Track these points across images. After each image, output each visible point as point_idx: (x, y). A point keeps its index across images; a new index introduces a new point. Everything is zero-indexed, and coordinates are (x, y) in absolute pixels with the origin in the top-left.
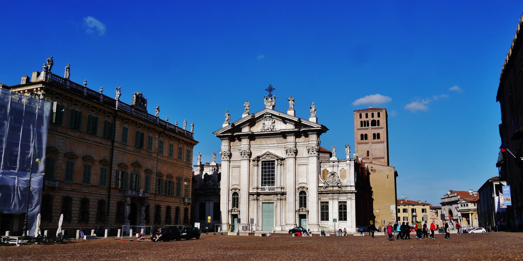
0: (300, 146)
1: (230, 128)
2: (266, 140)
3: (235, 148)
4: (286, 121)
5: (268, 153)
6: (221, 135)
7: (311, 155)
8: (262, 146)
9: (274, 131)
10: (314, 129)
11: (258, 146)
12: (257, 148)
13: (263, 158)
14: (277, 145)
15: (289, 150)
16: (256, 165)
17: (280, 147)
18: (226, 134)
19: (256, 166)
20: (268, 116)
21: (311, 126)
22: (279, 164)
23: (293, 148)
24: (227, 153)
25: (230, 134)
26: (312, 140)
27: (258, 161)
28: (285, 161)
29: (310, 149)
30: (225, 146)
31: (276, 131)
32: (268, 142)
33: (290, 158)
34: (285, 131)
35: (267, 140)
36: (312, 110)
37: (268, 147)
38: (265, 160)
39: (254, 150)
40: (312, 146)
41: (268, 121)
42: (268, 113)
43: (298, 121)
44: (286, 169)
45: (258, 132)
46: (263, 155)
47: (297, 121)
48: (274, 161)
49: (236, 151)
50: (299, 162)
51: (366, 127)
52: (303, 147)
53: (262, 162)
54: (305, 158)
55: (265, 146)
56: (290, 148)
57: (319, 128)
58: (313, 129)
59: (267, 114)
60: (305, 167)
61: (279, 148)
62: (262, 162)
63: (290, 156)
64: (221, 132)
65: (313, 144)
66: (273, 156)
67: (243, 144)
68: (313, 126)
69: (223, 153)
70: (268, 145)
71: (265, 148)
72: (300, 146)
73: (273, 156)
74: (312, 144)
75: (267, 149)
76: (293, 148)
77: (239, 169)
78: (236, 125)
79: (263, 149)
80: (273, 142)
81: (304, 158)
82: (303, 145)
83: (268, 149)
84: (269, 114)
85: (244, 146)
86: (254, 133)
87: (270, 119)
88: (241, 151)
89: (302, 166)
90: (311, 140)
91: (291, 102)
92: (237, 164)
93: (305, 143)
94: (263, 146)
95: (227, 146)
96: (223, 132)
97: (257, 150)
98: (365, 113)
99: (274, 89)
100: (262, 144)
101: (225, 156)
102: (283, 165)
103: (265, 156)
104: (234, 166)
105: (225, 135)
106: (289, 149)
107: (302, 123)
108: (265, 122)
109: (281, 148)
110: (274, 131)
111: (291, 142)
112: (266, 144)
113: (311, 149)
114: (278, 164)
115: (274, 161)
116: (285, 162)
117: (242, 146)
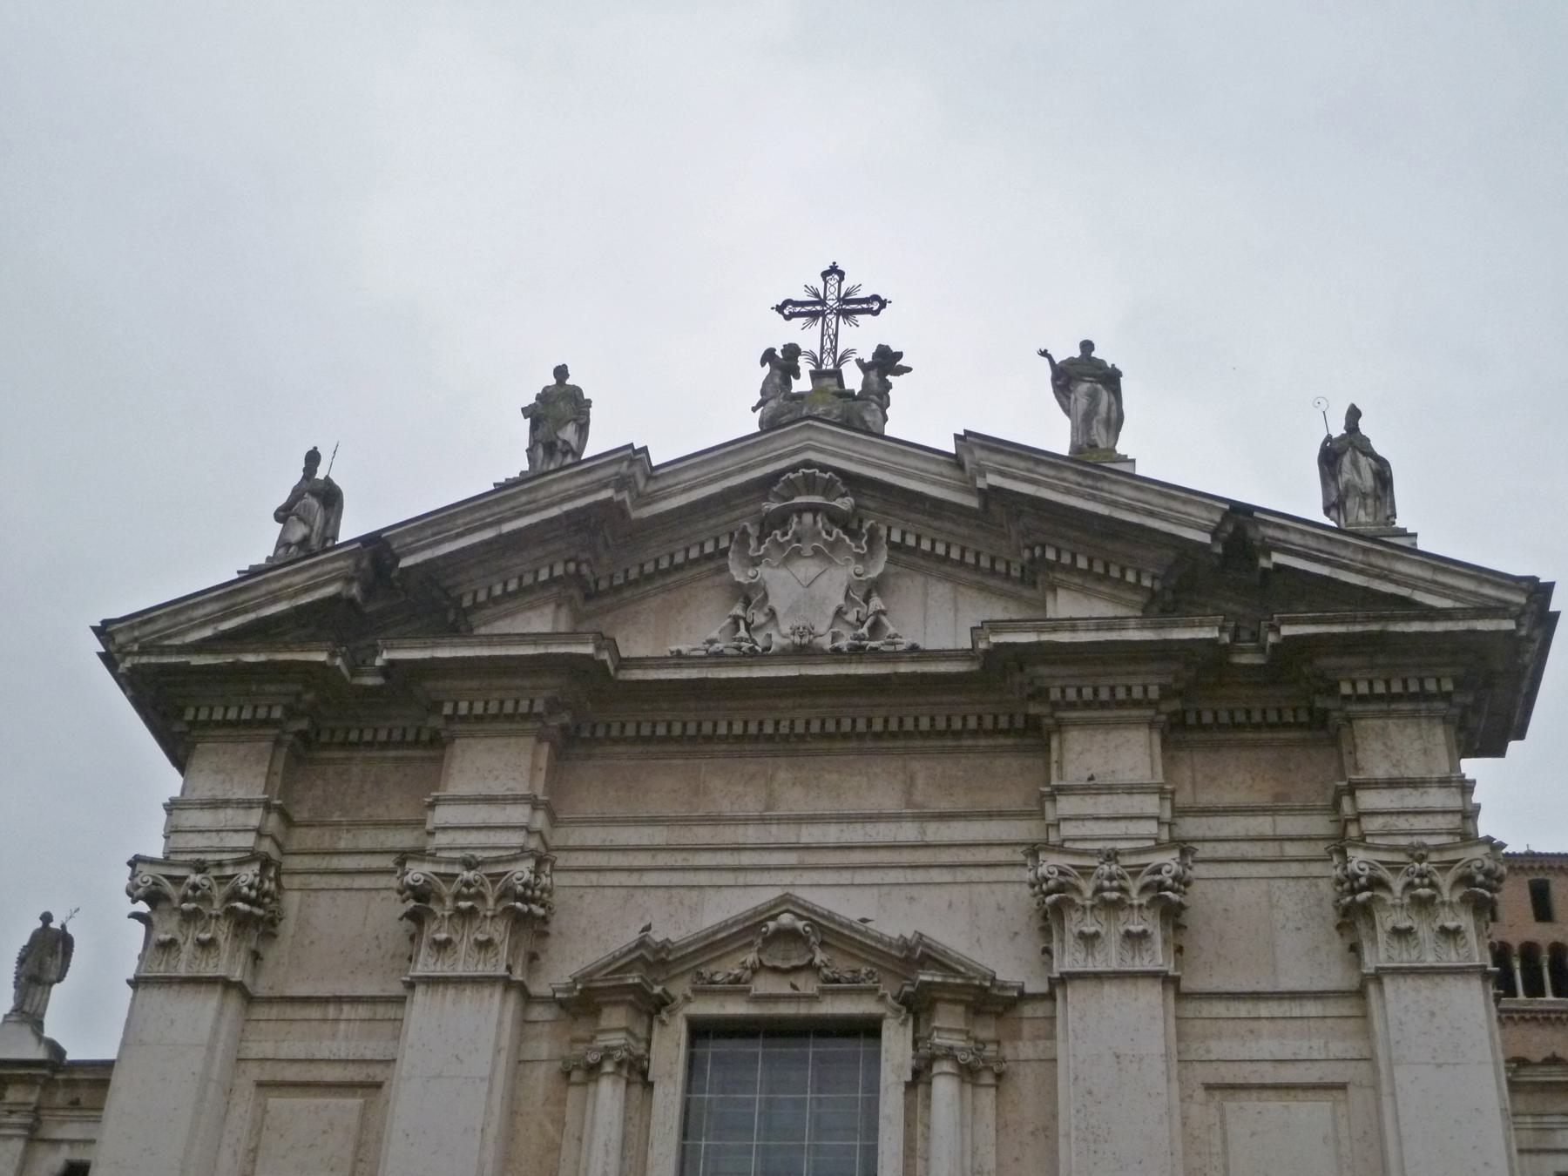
0: (1223, 850)
1: (330, 590)
2: (772, 778)
3: (342, 845)
4: (1051, 555)
5: (786, 919)
6: (197, 660)
7: (1404, 956)
8: (703, 835)
9: (895, 657)
10: (1439, 627)
11: (659, 836)
12: (643, 860)
13: (706, 989)
14: (908, 832)
15: (1087, 887)
16: (608, 1053)
17: (946, 857)
18: (262, 658)
19: (608, 1067)
20: (814, 509)
21: (1393, 596)
22: (949, 1054)
23: (1156, 859)
24: (226, 889)
25: (322, 657)
26: (1395, 773)
27: (653, 1007)
28: (1016, 1036)
29: (1384, 873)
30: (215, 804)
31: (915, 653)
32: (795, 799)
33: (1110, 990)
34: (1045, 637)
35: (782, 775)
36: (1346, 475)
37: (791, 858)
38: (736, 1008)
39: (594, 878)
40: (1403, 841)
41: (806, 569)
42: (824, 468)
43: (1214, 534)
44: (1048, 1130)
45: (679, 659)
46: (714, 945)
47: (1206, 538)
48: (870, 1029)
49: (346, 882)
50: (1218, 1049)
51: (1550, 997)
52: (1262, 869)
53: (701, 1031)
54: (1312, 1008)
55: (751, 834)
56: (1112, 856)
57: (1509, 625)
58: (1416, 627)
59: (810, 485)
60: (1313, 1113)
61: (935, 875)
62: (701, 1031)
63: (1110, 957)
64: (208, 632)
65: (1419, 823)
66: (843, 966)
67: (458, 784)
68: (1419, 596)
69: (169, 888)
70: (786, 834)
71: (747, 859)
72: (1223, 850)
73: (843, 966)
74: (1402, 823)
75: (765, 878)
76: (1156, 859)
77: (365, 1109)
78: (405, 563)
79: (728, 878)
80: (849, 805)
81: (1294, 1009)
82: (1271, 850)
83: (787, 878)
84: (827, 489)
85: (481, 814)
86: (638, 675)
87: (833, 546)
88: (428, 868)
89: (1273, 1106)
90: (1381, 771)
91: (1093, 397)
92: (341, 1049)
93: (1289, 825)
94: (728, 835)
95: (248, 805)
96: (226, 626)
97: (634, 879)
98: (1525, 879)
99: (874, 305)
100: (716, 820)
101: (190, 917)
102: (987, 1078)
103: (751, 957)
104: (291, 1073)
105: (250, 658)
106: (1085, 872)
107: (1278, 558)
108: (764, 572)
109: (961, 876)
110: (895, 657)
111: (1110, 789)
112: (763, 820)
113: (1397, 883)
114: (920, 1078)
115: (870, 1029)
116: (1026, 1049)
117: (443, 815)
